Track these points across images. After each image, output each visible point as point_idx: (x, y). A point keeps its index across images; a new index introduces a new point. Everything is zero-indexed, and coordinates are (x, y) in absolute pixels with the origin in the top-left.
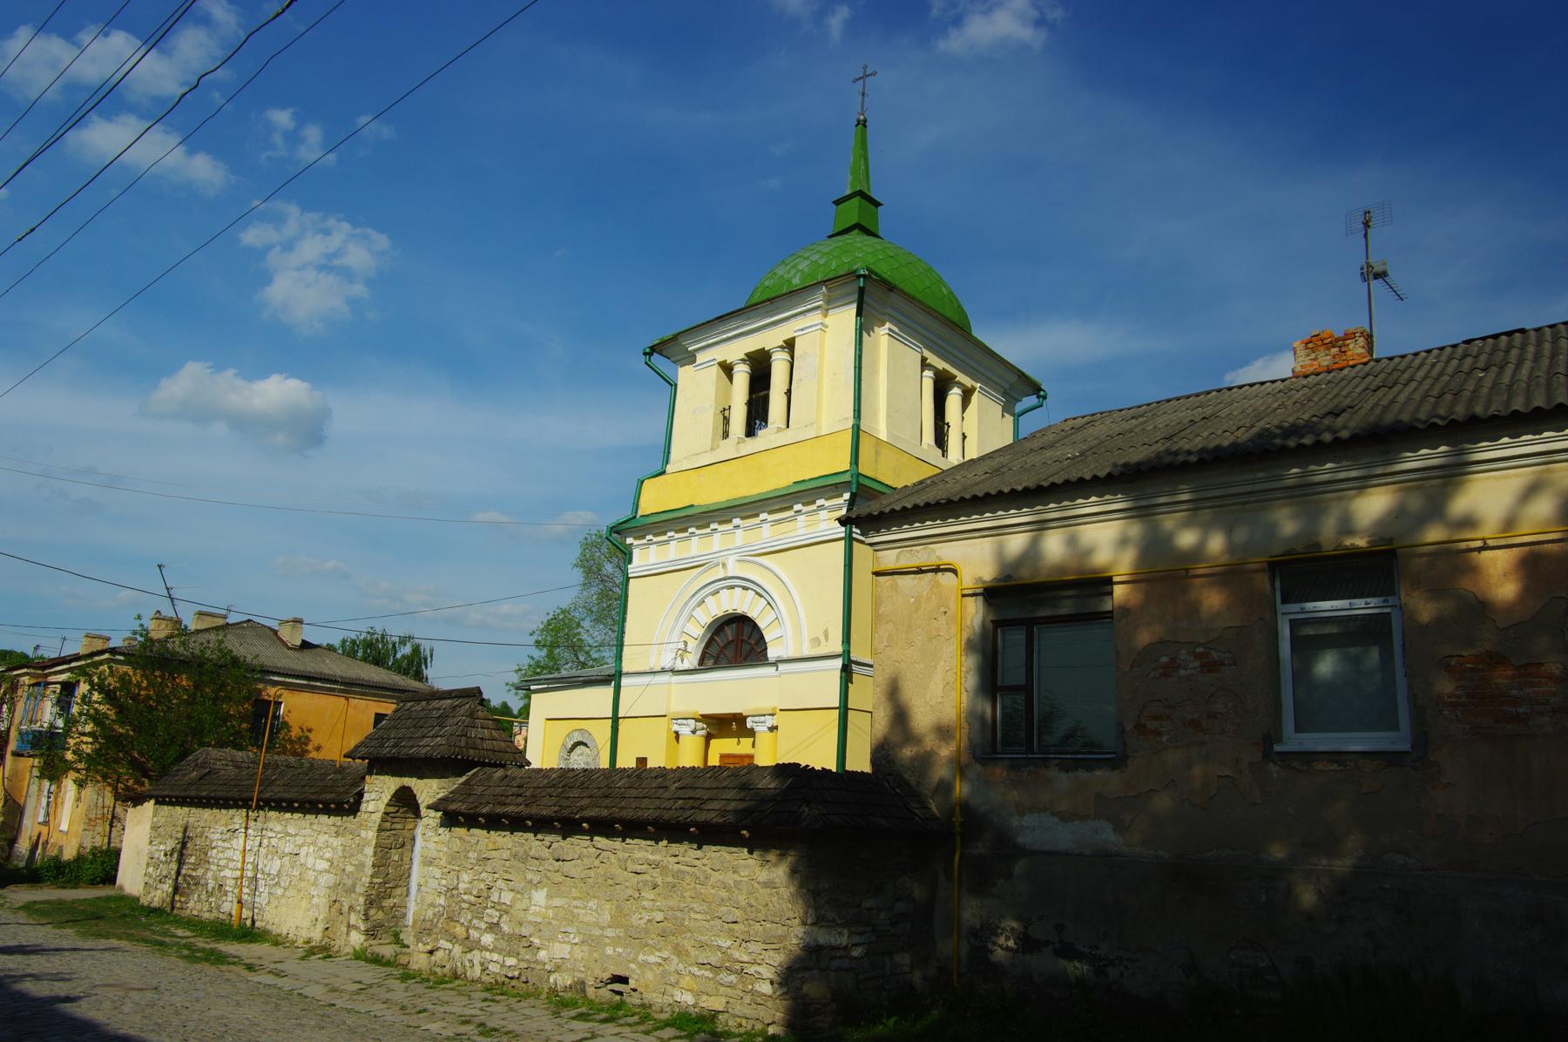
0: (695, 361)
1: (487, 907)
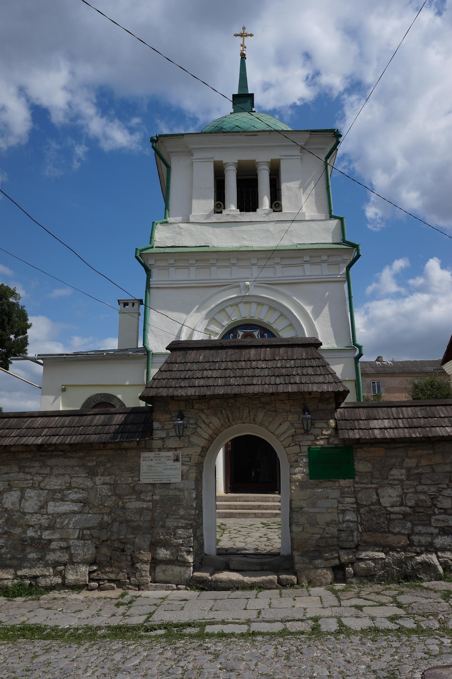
0: (192, 156)
1: (435, 514)
